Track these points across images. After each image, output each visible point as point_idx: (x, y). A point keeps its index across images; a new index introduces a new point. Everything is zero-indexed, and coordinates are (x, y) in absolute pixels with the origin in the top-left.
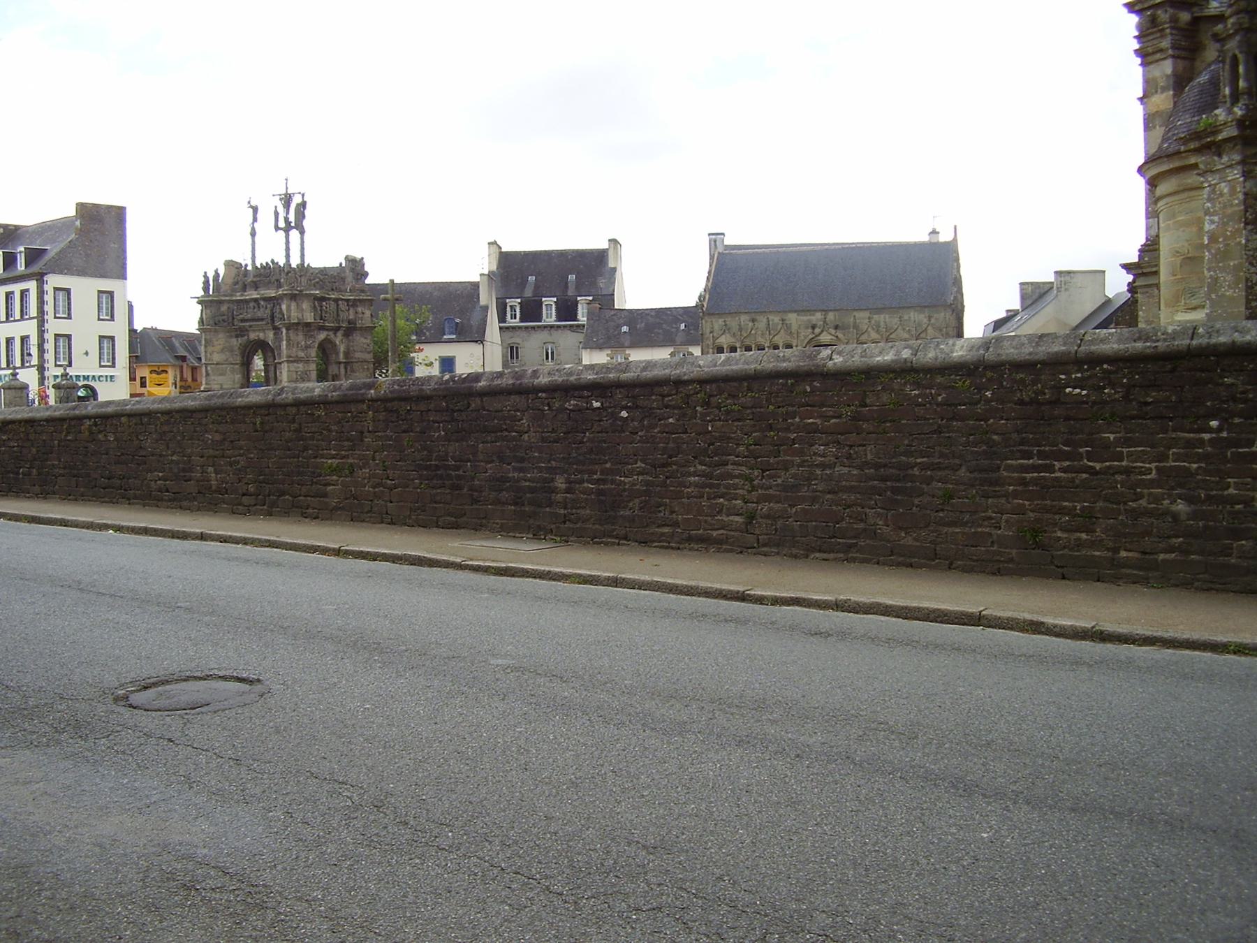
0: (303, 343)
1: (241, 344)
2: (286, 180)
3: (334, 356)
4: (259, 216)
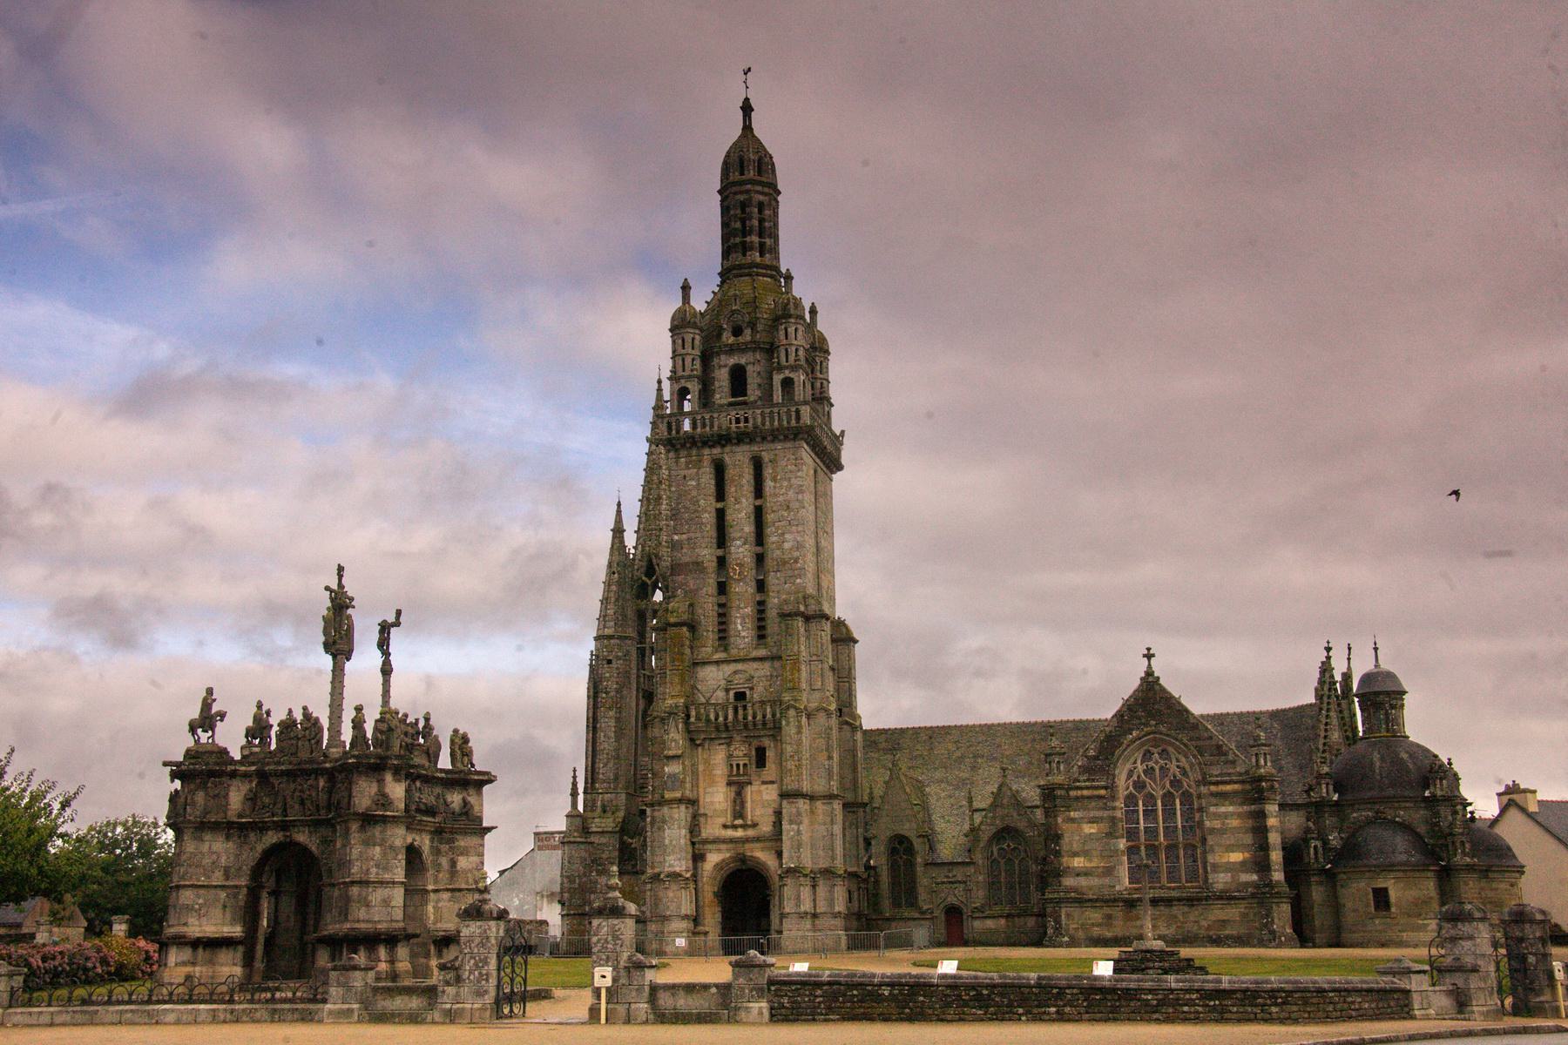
2: (340, 569)
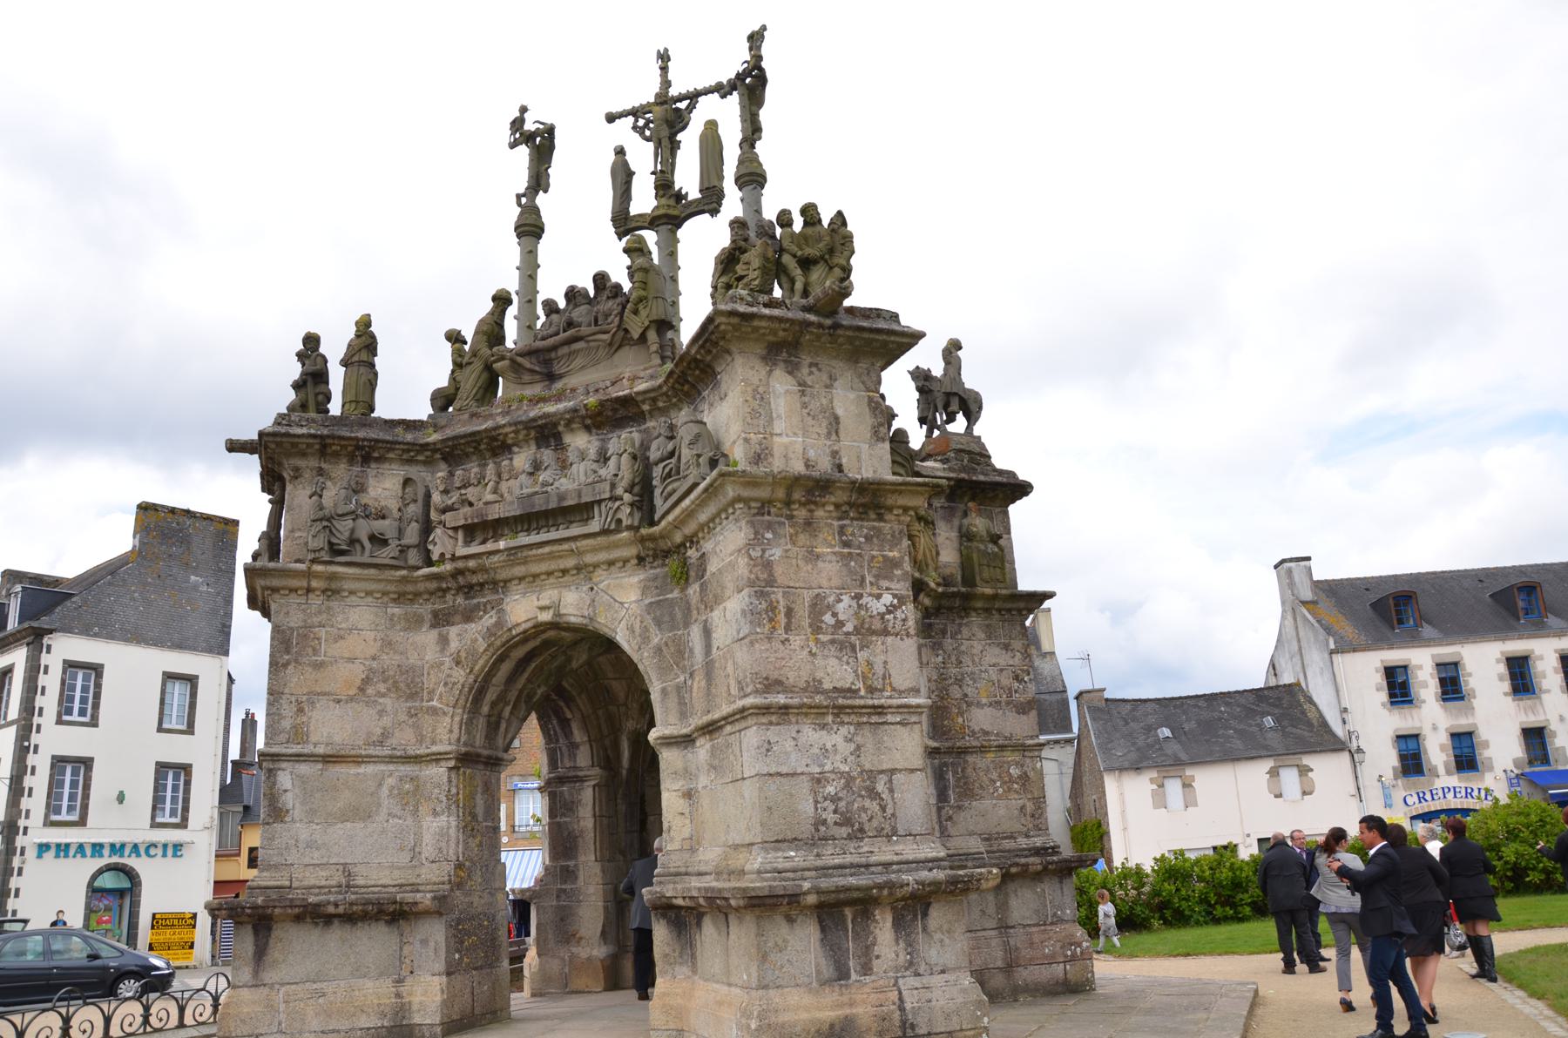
0: (845, 607)
2: (664, 57)
4: (557, 170)
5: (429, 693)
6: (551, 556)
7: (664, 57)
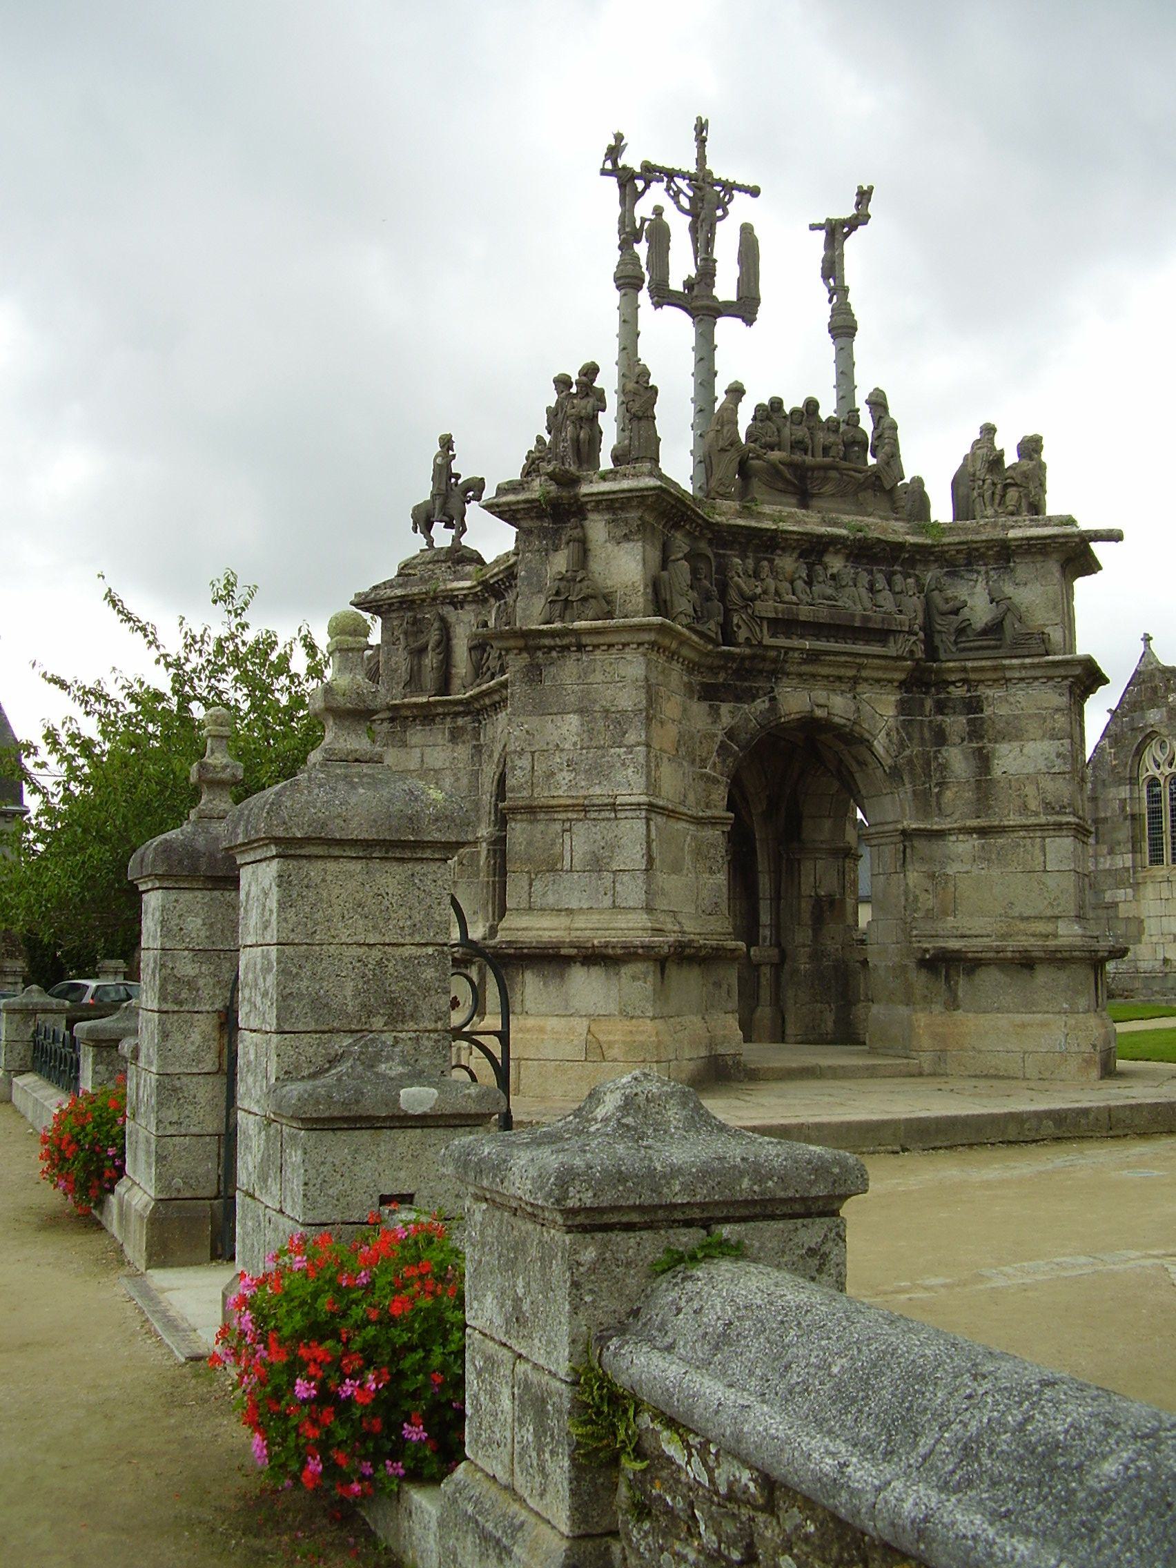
1: (731, 734)
2: (701, 128)
3: (827, 824)
5: (702, 760)
6: (844, 665)
7: (701, 128)
